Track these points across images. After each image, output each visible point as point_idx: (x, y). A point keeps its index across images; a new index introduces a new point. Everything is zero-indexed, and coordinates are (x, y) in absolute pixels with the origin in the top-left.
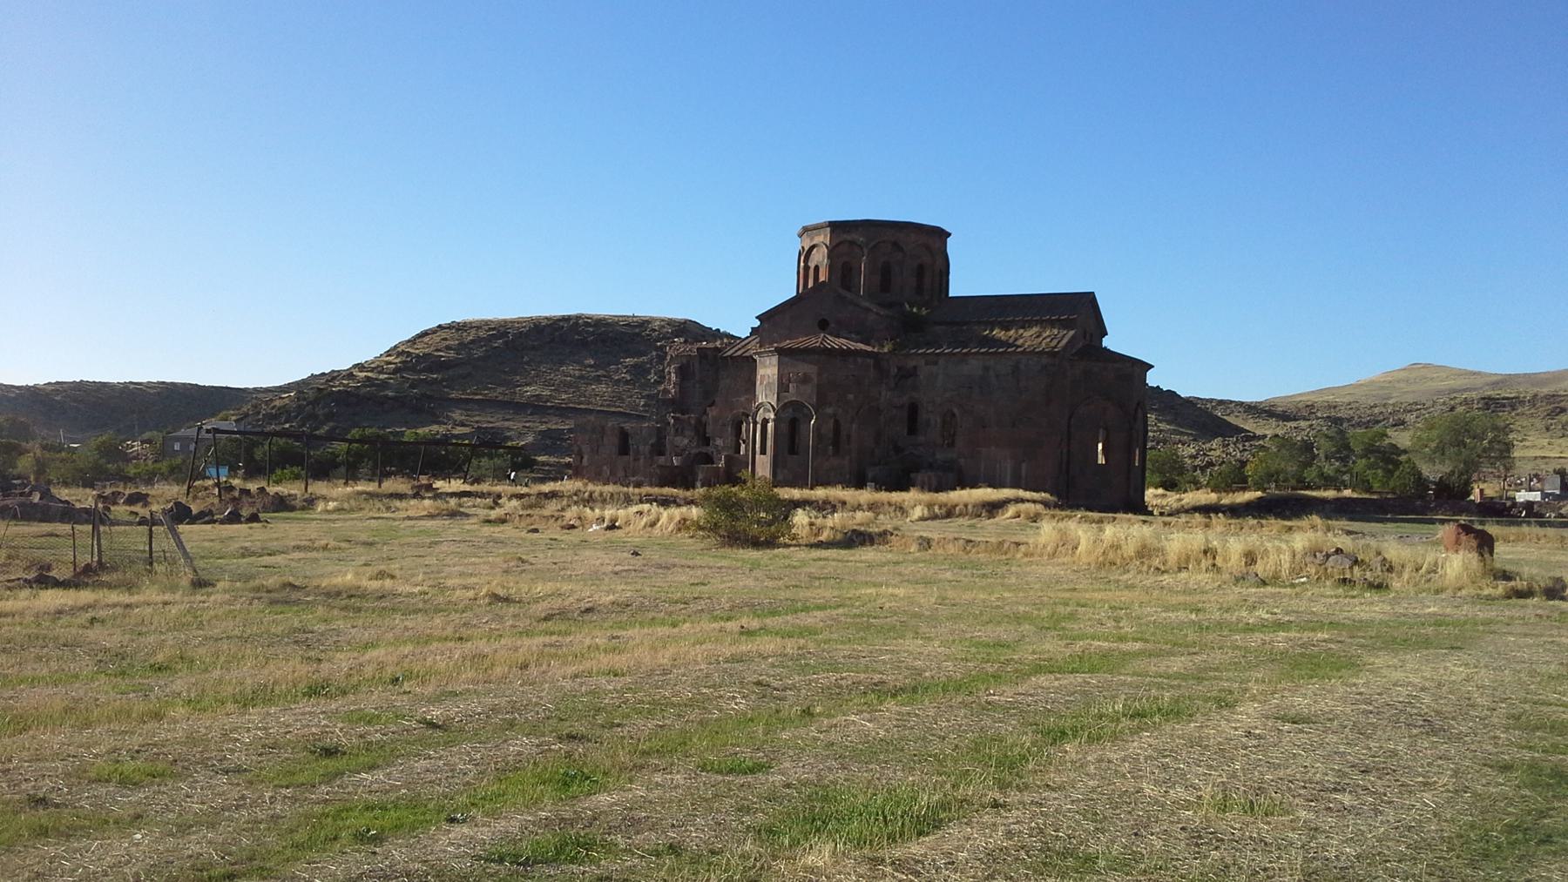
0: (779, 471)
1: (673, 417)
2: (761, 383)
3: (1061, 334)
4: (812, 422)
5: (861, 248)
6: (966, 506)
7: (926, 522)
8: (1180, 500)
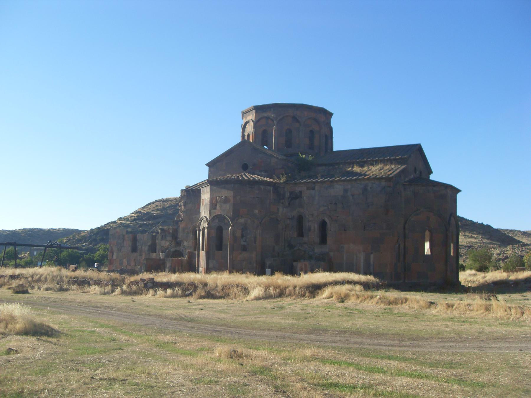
0: (210, 261)
1: (160, 228)
2: (202, 205)
3: (397, 168)
4: (230, 229)
5: (272, 120)
6: (295, 287)
7: (261, 301)
8: (485, 277)
